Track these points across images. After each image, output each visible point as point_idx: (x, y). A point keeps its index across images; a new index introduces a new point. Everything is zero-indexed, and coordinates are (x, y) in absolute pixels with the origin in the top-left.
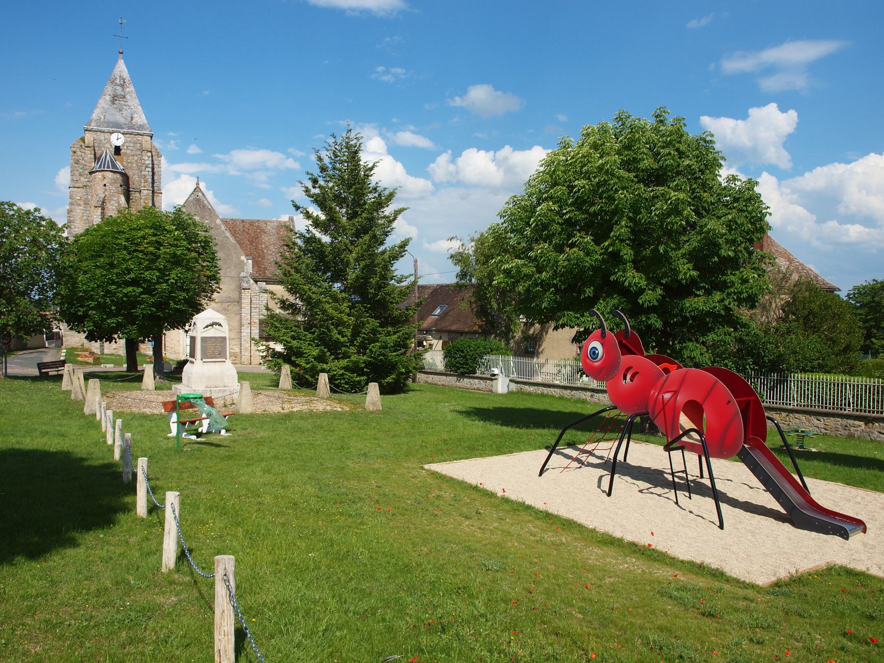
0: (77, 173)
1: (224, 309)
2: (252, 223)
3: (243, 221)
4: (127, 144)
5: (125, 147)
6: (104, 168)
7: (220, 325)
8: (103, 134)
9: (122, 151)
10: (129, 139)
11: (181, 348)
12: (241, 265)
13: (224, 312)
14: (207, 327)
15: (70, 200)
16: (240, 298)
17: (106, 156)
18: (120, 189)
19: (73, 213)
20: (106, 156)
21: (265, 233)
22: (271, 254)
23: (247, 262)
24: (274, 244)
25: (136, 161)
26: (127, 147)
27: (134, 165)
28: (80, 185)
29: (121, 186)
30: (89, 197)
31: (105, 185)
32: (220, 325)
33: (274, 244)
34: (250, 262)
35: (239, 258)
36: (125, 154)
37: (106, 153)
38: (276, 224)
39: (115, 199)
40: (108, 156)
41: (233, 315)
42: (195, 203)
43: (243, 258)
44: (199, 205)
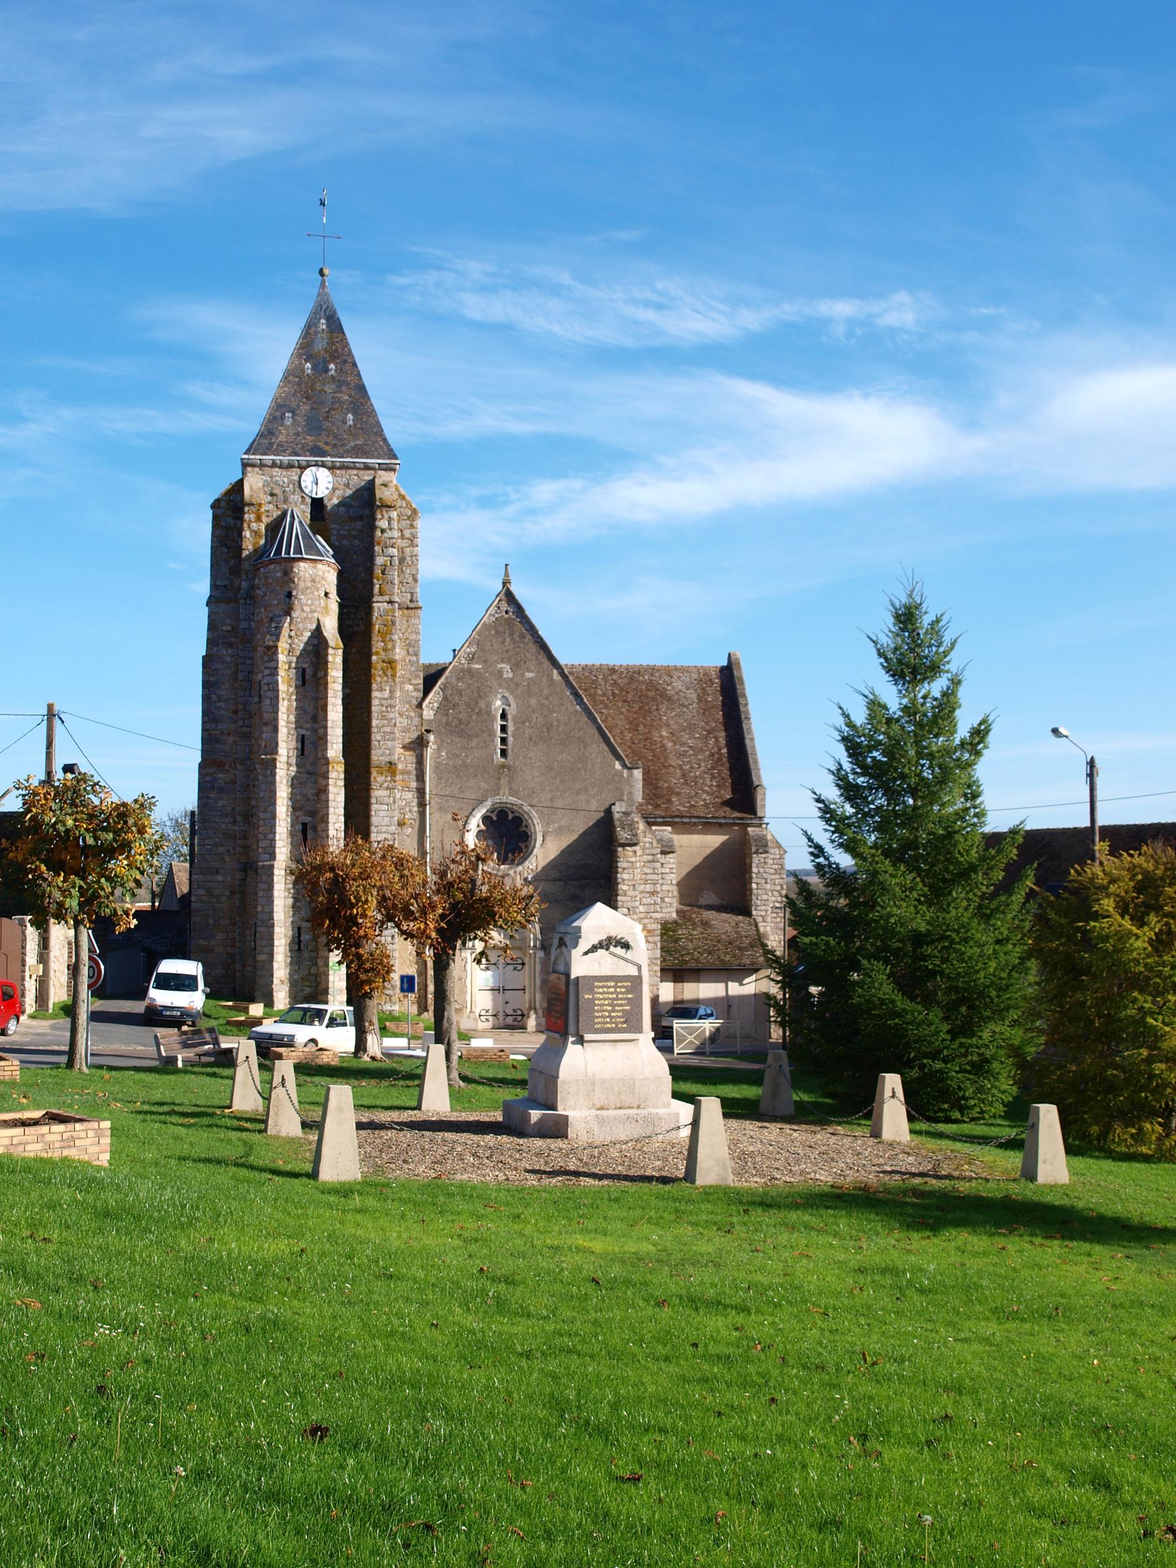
2: (634, 674)
3: (613, 670)
6: (288, 552)
7: (626, 946)
14: (594, 949)
22: (684, 754)
23: (631, 775)
24: (691, 728)
30: (253, 624)
32: (626, 946)
34: (638, 774)
38: (696, 676)
40: (296, 523)
43: (618, 766)
44: (512, 634)
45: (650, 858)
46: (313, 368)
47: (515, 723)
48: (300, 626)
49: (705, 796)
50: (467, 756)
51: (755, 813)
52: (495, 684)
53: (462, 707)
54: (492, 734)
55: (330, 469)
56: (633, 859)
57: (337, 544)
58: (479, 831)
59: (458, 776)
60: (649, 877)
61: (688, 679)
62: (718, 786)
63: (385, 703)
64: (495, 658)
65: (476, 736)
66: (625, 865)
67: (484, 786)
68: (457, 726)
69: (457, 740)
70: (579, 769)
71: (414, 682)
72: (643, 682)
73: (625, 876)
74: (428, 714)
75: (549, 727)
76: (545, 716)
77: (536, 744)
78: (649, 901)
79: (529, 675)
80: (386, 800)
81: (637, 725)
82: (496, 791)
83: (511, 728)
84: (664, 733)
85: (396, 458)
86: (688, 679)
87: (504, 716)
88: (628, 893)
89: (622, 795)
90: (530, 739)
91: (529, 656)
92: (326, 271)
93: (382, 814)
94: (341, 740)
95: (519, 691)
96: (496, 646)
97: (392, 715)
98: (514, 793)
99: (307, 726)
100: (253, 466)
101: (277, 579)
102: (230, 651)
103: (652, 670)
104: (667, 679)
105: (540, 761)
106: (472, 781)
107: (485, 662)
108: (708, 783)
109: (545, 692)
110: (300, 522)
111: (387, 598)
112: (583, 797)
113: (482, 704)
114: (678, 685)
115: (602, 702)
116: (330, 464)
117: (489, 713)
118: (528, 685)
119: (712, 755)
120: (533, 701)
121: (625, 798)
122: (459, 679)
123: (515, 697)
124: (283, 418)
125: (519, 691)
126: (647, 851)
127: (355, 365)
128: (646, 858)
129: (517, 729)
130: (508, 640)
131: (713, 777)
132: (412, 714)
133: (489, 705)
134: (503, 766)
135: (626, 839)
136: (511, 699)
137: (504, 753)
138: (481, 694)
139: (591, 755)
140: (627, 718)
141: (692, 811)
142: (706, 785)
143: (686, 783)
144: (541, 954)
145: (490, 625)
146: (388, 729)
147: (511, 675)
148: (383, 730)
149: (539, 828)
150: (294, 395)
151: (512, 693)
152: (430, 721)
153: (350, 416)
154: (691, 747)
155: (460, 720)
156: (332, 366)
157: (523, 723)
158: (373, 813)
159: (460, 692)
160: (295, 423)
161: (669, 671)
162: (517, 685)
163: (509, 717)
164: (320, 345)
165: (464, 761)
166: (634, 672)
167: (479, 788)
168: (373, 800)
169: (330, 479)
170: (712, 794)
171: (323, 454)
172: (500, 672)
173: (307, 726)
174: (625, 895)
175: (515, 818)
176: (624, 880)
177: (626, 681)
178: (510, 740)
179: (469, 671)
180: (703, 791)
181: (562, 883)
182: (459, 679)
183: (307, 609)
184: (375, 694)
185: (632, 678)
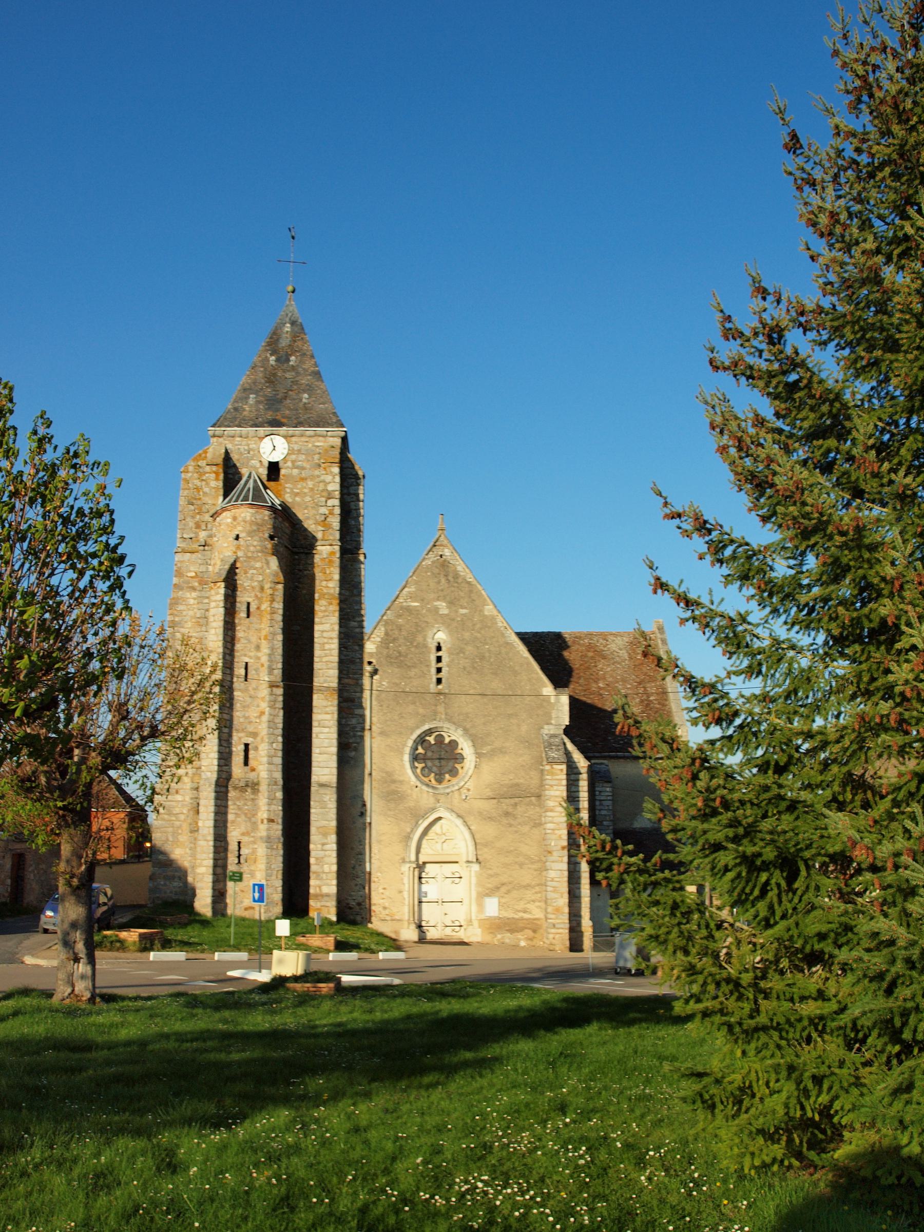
0: (191, 524)
1: (507, 814)
4: (293, 457)
5: (289, 464)
9: (283, 472)
10: (296, 447)
13: (505, 821)
15: (175, 580)
16: (542, 786)
17: (247, 482)
18: (269, 545)
19: (180, 607)
20: (247, 482)
21: (604, 658)
23: (558, 701)
25: (312, 490)
26: (293, 462)
27: (308, 499)
28: (195, 546)
29: (272, 537)
30: (211, 568)
31: (237, 538)
33: (624, 680)
36: (289, 477)
37: (249, 477)
39: (258, 565)
40: (251, 481)
41: (525, 829)
44: (446, 576)
46: (277, 360)
47: (450, 653)
54: (428, 666)
55: (285, 437)
59: (398, 703)
63: (325, 634)
64: (432, 596)
65: (414, 667)
67: (421, 711)
68: (396, 658)
69: (396, 670)
72: (583, 645)
73: (552, 793)
75: (482, 658)
77: (469, 673)
80: (327, 723)
83: (445, 660)
84: (601, 685)
85: (342, 426)
87: (439, 648)
89: (551, 718)
90: (464, 668)
91: (462, 594)
92: (290, 288)
93: (322, 736)
94: (280, 666)
101: (227, 525)
102: (194, 594)
103: (590, 635)
110: (255, 481)
113: (420, 639)
114: (613, 647)
117: (425, 646)
119: (642, 701)
120: (467, 635)
122: (400, 616)
124: (247, 398)
127: (312, 357)
129: (452, 661)
130: (443, 580)
134: (439, 693)
137: (439, 681)
138: (420, 628)
144: (476, 867)
147: (446, 611)
148: (324, 659)
152: (371, 654)
155: (399, 653)
156: (293, 358)
158: (314, 735)
159: (400, 628)
160: (258, 402)
161: (604, 636)
162: (453, 620)
163: (443, 648)
167: (418, 713)
168: (315, 724)
169: (286, 445)
172: (437, 609)
173: (252, 654)
174: (552, 811)
175: (451, 742)
179: (408, 609)
181: (495, 801)
184: (317, 627)
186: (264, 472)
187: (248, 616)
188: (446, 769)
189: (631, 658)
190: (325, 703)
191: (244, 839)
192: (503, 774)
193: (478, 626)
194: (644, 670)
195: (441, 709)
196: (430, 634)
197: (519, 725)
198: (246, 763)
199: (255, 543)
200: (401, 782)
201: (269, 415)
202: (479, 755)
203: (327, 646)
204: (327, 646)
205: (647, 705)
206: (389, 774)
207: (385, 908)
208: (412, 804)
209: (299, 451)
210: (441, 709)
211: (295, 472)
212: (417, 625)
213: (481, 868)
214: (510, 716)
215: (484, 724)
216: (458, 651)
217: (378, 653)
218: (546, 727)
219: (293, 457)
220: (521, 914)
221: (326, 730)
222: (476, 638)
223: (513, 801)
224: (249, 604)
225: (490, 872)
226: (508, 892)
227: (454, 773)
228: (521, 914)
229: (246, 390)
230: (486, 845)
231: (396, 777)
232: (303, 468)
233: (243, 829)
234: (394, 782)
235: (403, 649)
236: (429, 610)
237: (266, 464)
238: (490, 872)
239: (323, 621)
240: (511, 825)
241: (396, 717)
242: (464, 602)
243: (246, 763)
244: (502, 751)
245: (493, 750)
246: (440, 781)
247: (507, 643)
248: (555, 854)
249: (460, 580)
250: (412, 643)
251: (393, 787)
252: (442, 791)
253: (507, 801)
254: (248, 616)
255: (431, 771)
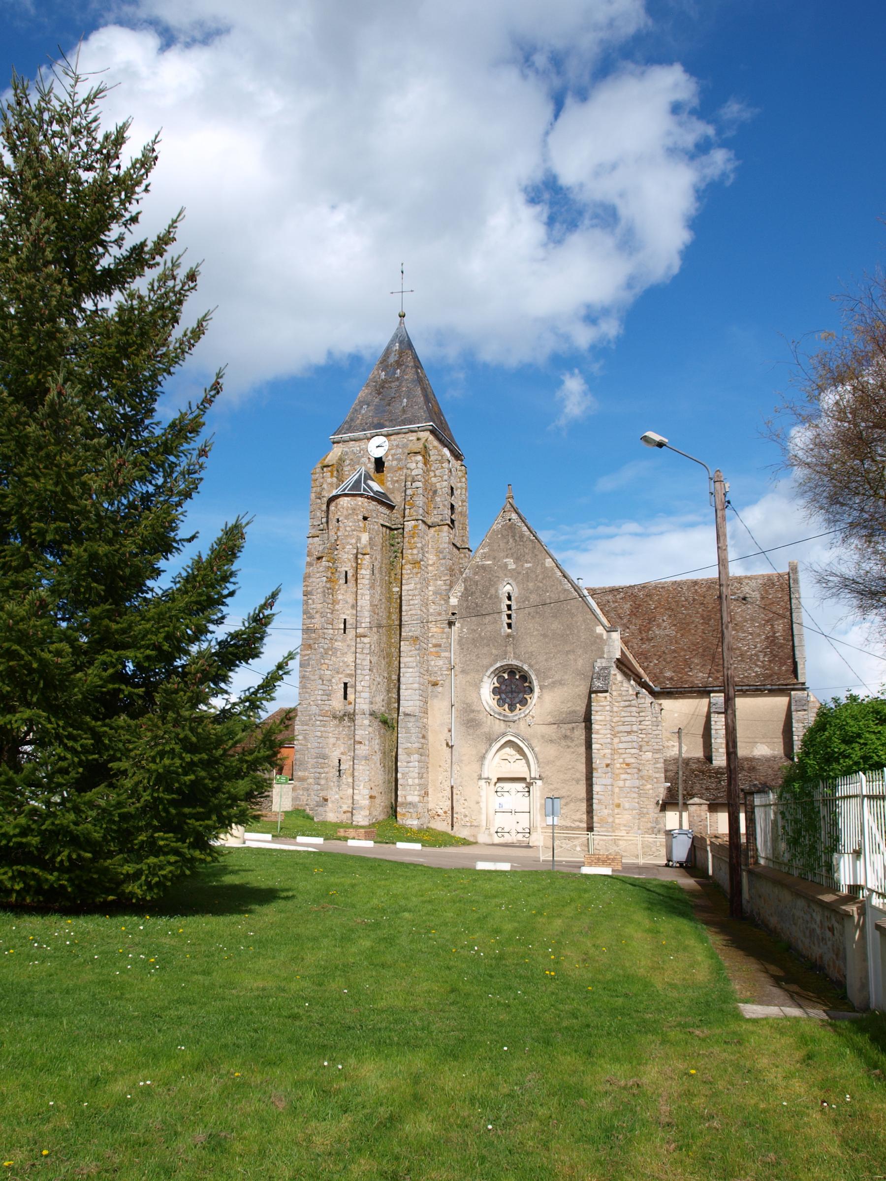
1: (566, 737)
4: (393, 452)
5: (390, 457)
8: (357, 444)
10: (395, 443)
11: (484, 817)
12: (597, 645)
13: (563, 743)
15: (308, 559)
22: (744, 639)
23: (609, 637)
33: (753, 620)
35: (593, 631)
36: (391, 467)
38: (761, 582)
42: (505, 533)
43: (599, 630)
44: (513, 536)
45: (627, 703)
47: (517, 602)
48: (344, 541)
49: (757, 669)
50: (482, 630)
51: (796, 677)
52: (501, 574)
53: (478, 594)
55: (387, 436)
56: (604, 703)
57: (391, 487)
58: (495, 688)
59: (475, 646)
60: (627, 719)
61: (754, 584)
62: (770, 661)
63: (410, 593)
66: (598, 708)
67: (494, 651)
68: (474, 609)
70: (567, 635)
71: (443, 578)
74: (454, 601)
76: (540, 595)
77: (533, 617)
78: (628, 738)
79: (528, 565)
81: (710, 620)
82: (504, 655)
86: (754, 584)
88: (601, 732)
89: (603, 653)
90: (529, 614)
91: (527, 551)
93: (408, 675)
95: (521, 577)
96: (502, 545)
97: (416, 602)
98: (517, 657)
99: (348, 612)
100: (338, 442)
104: (738, 585)
105: (538, 630)
106: (486, 649)
107: (494, 558)
108: (761, 659)
109: (540, 577)
111: (414, 518)
112: (571, 657)
113: (492, 591)
115: (683, 606)
116: (385, 433)
117: (497, 597)
118: (527, 573)
119: (767, 638)
120: (531, 585)
121: (605, 656)
122: (476, 573)
123: (517, 583)
125: (521, 577)
126: (625, 698)
128: (623, 704)
130: (511, 541)
131: (765, 656)
132: (443, 602)
133: (497, 592)
134: (509, 636)
135: (599, 687)
136: (514, 584)
137: (509, 626)
138: (492, 582)
139: (577, 622)
140: (702, 616)
141: (745, 680)
142: (758, 660)
143: (741, 661)
145: (498, 531)
146: (413, 612)
147: (514, 567)
149: (535, 683)
150: (370, 394)
151: (515, 580)
153: (405, 400)
154: (751, 634)
155: (476, 604)
157: (524, 601)
159: (476, 583)
162: (519, 573)
163: (513, 598)
164: (392, 359)
165: (480, 635)
166: (712, 583)
167: (491, 654)
170: (763, 667)
171: (382, 426)
172: (506, 565)
173: (348, 612)
174: (597, 733)
176: (597, 720)
177: (704, 589)
178: (514, 616)
179: (484, 567)
180: (757, 665)
181: (556, 726)
182: (476, 573)
183: (348, 529)
185: (709, 587)
186: (371, 466)
187: (346, 582)
188: (517, 700)
189: (762, 598)
190: (409, 648)
191: (343, 758)
192: (563, 702)
193: (540, 577)
194: (774, 609)
195: (510, 649)
196: (501, 586)
197: (575, 660)
198: (345, 698)
199: (351, 524)
200: (479, 711)
201: (376, 421)
202: (541, 688)
203: (412, 602)
204: (412, 602)
205: (773, 641)
206: (469, 705)
207: (466, 816)
208: (486, 730)
209: (397, 446)
210: (510, 649)
211: (395, 463)
212: (490, 580)
213: (544, 784)
214: (568, 652)
215: (546, 660)
216: (524, 599)
217: (460, 605)
218: (598, 660)
219: (393, 452)
220: (577, 824)
221: (411, 670)
222: (538, 587)
223: (570, 726)
224: (346, 572)
225: (551, 787)
226: (566, 804)
227: (524, 702)
228: (577, 824)
229: (361, 403)
230: (548, 763)
231: (474, 707)
232: (399, 460)
233: (342, 749)
234: (473, 711)
235: (479, 601)
236: (500, 567)
237: (373, 460)
238: (551, 787)
239: (409, 581)
240: (569, 747)
241: (474, 658)
242: (528, 557)
243: (345, 698)
244: (561, 683)
245: (554, 683)
246: (512, 708)
247: (565, 590)
248: (599, 770)
249: (525, 539)
250: (486, 595)
251: (472, 715)
252: (511, 719)
253: (566, 726)
254: (346, 582)
255: (504, 702)
